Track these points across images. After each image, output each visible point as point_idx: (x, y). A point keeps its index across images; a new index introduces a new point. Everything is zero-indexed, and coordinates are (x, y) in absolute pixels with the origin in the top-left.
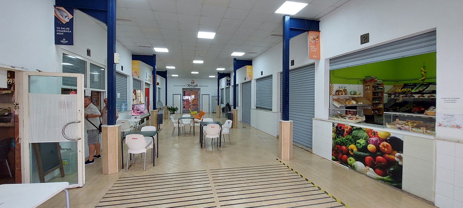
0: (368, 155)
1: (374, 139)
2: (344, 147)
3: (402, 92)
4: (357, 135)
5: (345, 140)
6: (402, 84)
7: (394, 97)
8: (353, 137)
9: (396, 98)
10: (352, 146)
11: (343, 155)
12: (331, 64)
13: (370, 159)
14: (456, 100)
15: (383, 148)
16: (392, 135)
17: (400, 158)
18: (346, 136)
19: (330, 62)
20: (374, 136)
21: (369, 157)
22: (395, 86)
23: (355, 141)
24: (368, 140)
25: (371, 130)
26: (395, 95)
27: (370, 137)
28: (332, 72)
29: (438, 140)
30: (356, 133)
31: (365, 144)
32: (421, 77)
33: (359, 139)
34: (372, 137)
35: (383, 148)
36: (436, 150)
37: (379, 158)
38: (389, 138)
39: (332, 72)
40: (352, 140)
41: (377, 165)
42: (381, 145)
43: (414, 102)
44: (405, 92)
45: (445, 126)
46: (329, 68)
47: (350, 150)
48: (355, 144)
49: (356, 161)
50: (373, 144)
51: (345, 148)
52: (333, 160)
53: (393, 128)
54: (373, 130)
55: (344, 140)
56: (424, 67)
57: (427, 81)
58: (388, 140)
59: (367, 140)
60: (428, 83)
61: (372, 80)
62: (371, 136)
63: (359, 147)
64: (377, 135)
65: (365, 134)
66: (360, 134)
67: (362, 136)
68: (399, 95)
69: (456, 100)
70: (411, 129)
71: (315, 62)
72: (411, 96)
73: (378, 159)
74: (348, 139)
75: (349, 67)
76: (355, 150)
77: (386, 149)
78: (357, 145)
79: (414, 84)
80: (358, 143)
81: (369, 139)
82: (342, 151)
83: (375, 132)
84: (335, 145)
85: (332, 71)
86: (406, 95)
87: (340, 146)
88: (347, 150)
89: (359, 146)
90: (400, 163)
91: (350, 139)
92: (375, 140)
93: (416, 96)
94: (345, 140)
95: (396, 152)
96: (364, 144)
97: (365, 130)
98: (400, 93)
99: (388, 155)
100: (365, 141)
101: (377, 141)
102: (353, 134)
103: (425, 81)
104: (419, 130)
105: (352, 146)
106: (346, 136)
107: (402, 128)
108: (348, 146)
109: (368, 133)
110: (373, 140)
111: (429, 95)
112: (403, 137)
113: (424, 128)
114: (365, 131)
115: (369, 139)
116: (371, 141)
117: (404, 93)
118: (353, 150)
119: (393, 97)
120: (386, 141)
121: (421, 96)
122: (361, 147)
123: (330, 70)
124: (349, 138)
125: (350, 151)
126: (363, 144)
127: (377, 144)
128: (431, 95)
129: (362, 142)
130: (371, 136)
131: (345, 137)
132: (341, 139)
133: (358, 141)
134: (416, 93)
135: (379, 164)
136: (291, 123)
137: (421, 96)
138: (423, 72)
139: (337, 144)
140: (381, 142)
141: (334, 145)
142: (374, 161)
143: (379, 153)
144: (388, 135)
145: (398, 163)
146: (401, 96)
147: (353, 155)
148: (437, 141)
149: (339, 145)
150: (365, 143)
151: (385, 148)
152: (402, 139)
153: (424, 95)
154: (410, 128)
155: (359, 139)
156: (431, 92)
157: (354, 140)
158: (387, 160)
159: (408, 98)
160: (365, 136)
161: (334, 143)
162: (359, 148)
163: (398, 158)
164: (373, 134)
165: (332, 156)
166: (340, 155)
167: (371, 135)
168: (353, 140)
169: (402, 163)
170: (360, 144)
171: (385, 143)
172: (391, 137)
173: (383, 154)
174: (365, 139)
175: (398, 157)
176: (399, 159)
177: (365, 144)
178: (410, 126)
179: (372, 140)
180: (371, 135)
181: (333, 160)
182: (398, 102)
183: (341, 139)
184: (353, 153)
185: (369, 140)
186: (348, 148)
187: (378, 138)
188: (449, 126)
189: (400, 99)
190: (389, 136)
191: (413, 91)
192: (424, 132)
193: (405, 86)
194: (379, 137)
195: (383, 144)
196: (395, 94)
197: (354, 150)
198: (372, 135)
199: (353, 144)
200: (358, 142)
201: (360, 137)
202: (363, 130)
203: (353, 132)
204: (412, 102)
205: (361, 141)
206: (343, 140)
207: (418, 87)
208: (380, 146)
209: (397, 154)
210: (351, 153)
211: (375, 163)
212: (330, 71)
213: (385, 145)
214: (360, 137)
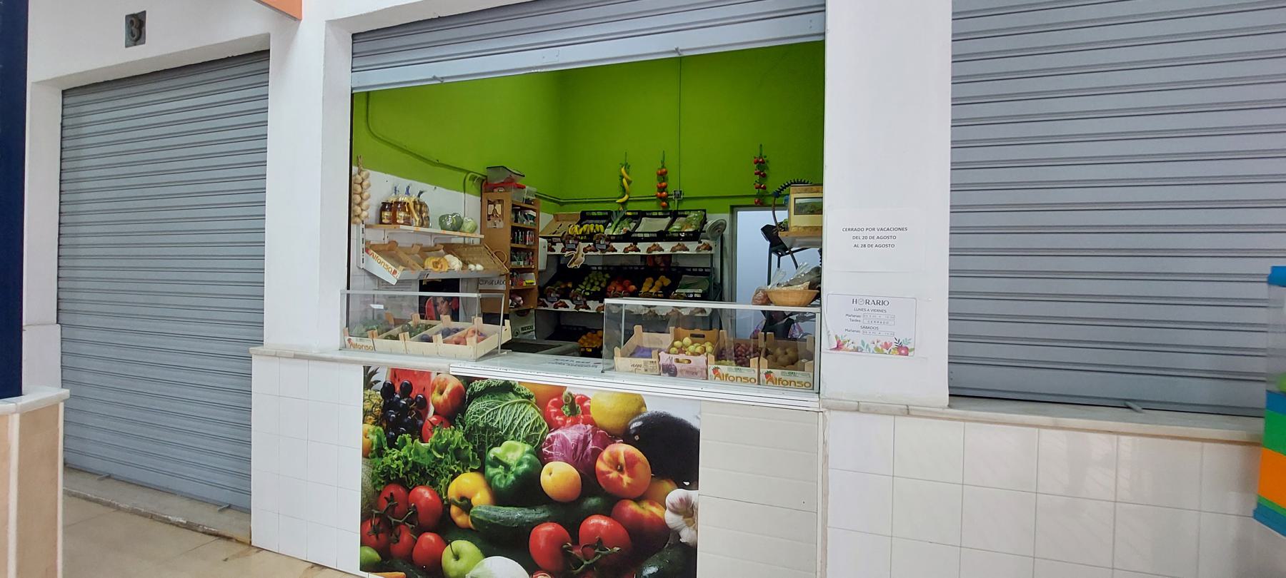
0: (542, 516)
1: (571, 434)
2: (425, 493)
3: (583, 234)
4: (492, 421)
5: (429, 452)
6: (577, 211)
7: (563, 250)
8: (468, 436)
9: (567, 253)
10: (468, 484)
11: (420, 531)
12: (359, 62)
13: (550, 537)
14: (895, 237)
15: (614, 474)
16: (652, 408)
17: (688, 510)
18: (436, 432)
19: (354, 66)
20: (569, 421)
21: (548, 528)
22: (557, 218)
23: (482, 456)
24: (543, 440)
25: (559, 391)
26: (564, 245)
27: (553, 426)
28: (362, 102)
29: (834, 413)
30: (484, 412)
31: (530, 462)
32: (620, 194)
33: (499, 441)
34: (564, 423)
35: (614, 474)
36: (826, 457)
37: (593, 524)
38: (640, 423)
39: (361, 105)
40: (466, 448)
41: (588, 561)
42: (602, 459)
43: (606, 268)
44: (592, 235)
45: (856, 350)
46: (346, 81)
47: (457, 505)
48: (481, 471)
49: (486, 556)
50: (566, 461)
51: (431, 494)
52: (367, 566)
53: (643, 369)
54: (566, 387)
55: (427, 455)
56: (627, 166)
57: (632, 206)
58: (633, 432)
59: (541, 443)
60: (639, 211)
61: (511, 182)
62: (557, 418)
63: (502, 484)
64: (586, 411)
65: (531, 414)
66: (505, 413)
67: (517, 423)
68: (576, 245)
69: (895, 237)
70: (767, 374)
71: (268, 36)
72: (608, 246)
73: (592, 529)
74: (443, 449)
75: (446, 81)
76: (481, 498)
77: (626, 479)
78: (491, 471)
79: (607, 214)
80: (497, 462)
81: (549, 436)
82: (415, 514)
83: (573, 399)
84: (375, 487)
85: (365, 95)
86: (594, 245)
87: (401, 490)
88: (440, 506)
89: (498, 477)
90: (686, 536)
91: (453, 446)
92: (578, 441)
93: (620, 248)
94: (429, 452)
95: (667, 485)
96: (525, 466)
97: (527, 392)
98: (577, 239)
99: (633, 507)
100: (528, 447)
101: (585, 442)
102: (470, 420)
103: (627, 207)
104: (745, 372)
105: (468, 484)
106: (436, 432)
107: (678, 366)
108: (443, 481)
109: (541, 404)
110: (568, 437)
111: (650, 244)
112: (700, 413)
113: (764, 361)
114: (529, 397)
115: (549, 436)
116: (556, 443)
117: (589, 237)
118: (469, 501)
119: (558, 248)
120: (627, 437)
121: (631, 248)
122: (509, 482)
123: (352, 89)
124: (448, 443)
125: (454, 510)
126: (520, 463)
127: (583, 460)
128: (654, 245)
129: (514, 453)
130: (557, 418)
131: (432, 439)
132: (412, 449)
133: (496, 452)
134: (619, 239)
135: (597, 554)
136: (31, 419)
137: (631, 248)
138: (624, 180)
139: (389, 482)
140: (605, 448)
141: (369, 485)
142: (572, 544)
143: (593, 501)
144: (633, 408)
145: (680, 538)
146: (583, 245)
147: (470, 529)
148: (832, 416)
149: (401, 482)
150: (528, 456)
151: (621, 471)
152: (694, 423)
153: (639, 245)
154: (711, 367)
155: (503, 440)
156: (656, 235)
157: (474, 450)
158: (630, 531)
159: (599, 253)
160: (532, 421)
161: (373, 477)
162: (502, 486)
163: (675, 511)
164: (566, 409)
165: (362, 544)
166: (406, 537)
167: (556, 414)
168: (471, 447)
169: (694, 532)
170: (507, 467)
171: (622, 449)
172: (646, 415)
173: (611, 501)
174: (527, 440)
175: (678, 506)
176: (681, 518)
177: (530, 462)
178: (712, 357)
179: (564, 442)
180: (556, 414)
181: (367, 566)
182: (573, 266)
183: (412, 449)
184: (472, 518)
185: (550, 442)
186: (446, 493)
187: (589, 427)
188: (872, 347)
189: (580, 256)
190: (640, 413)
191: (609, 231)
192: (763, 376)
193: (585, 217)
194: (592, 422)
195: (611, 454)
196: (565, 239)
197: (474, 501)
198: (561, 414)
199: (472, 470)
200: (496, 459)
201: (507, 433)
202: (517, 394)
203: (472, 408)
204: (599, 268)
205: (508, 449)
206: (417, 453)
207: (618, 223)
208: (601, 466)
209: (676, 495)
210: (462, 520)
211: (577, 552)
212: (352, 95)
213: (622, 460)
214: (507, 433)
